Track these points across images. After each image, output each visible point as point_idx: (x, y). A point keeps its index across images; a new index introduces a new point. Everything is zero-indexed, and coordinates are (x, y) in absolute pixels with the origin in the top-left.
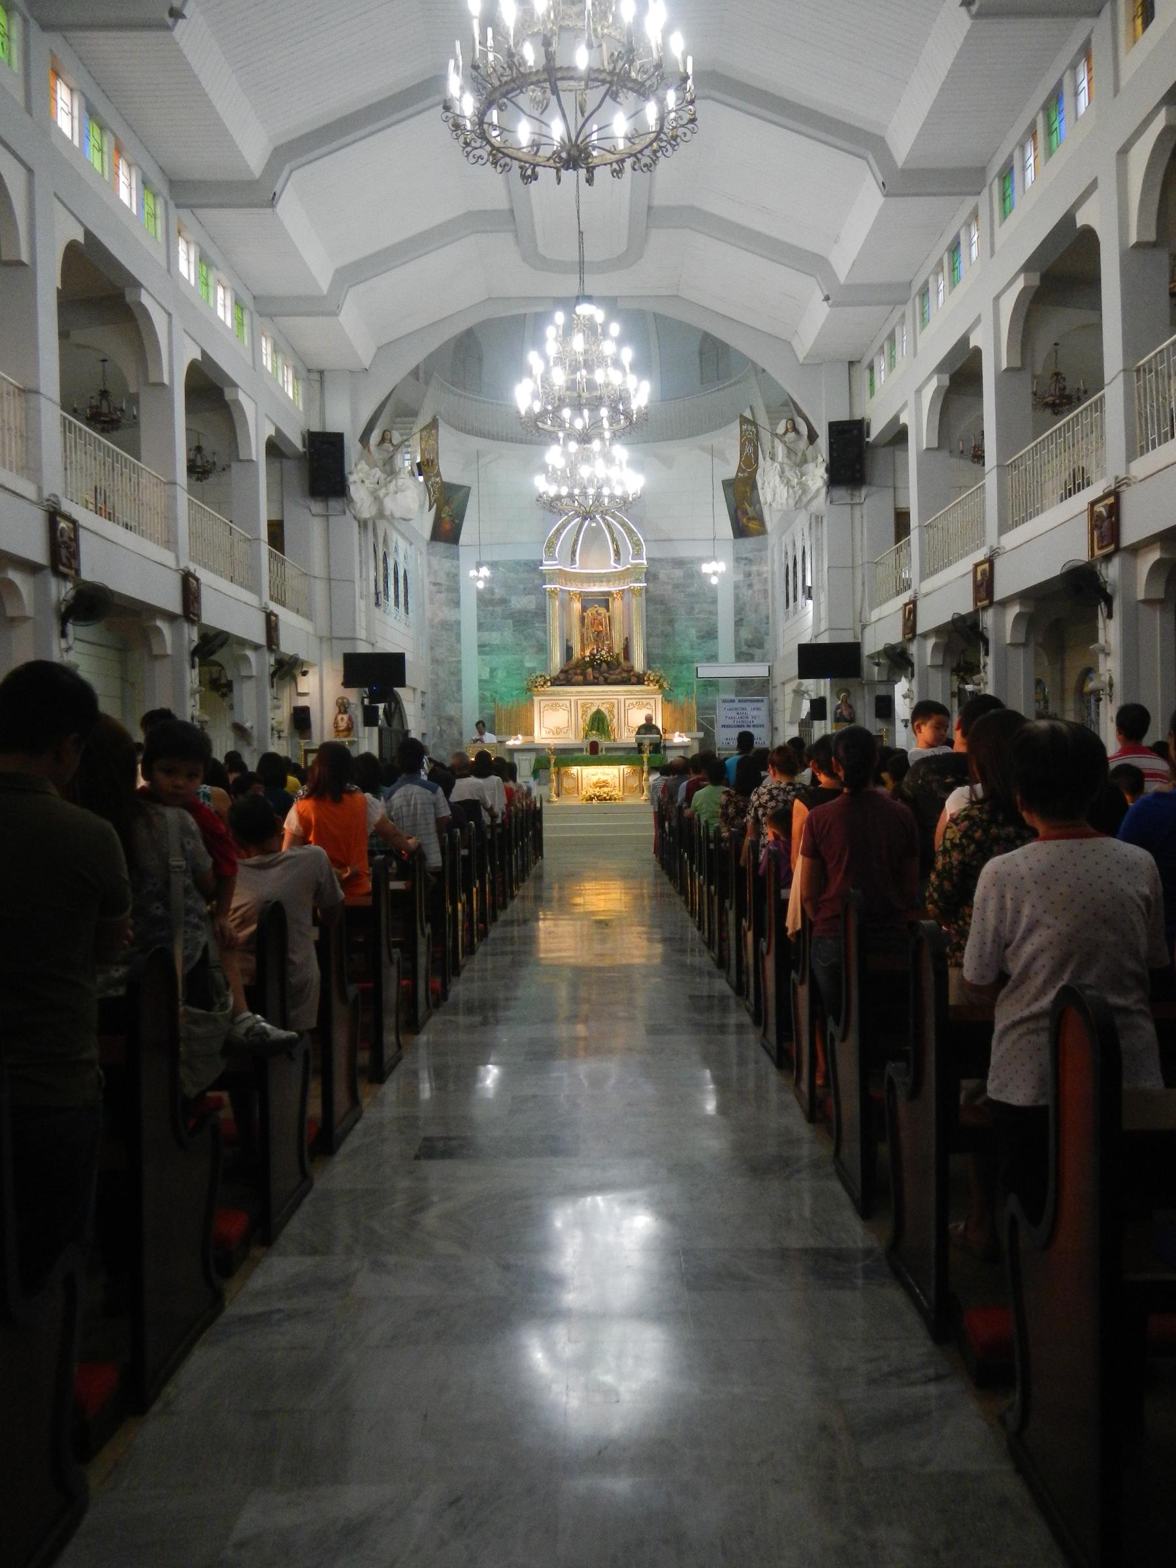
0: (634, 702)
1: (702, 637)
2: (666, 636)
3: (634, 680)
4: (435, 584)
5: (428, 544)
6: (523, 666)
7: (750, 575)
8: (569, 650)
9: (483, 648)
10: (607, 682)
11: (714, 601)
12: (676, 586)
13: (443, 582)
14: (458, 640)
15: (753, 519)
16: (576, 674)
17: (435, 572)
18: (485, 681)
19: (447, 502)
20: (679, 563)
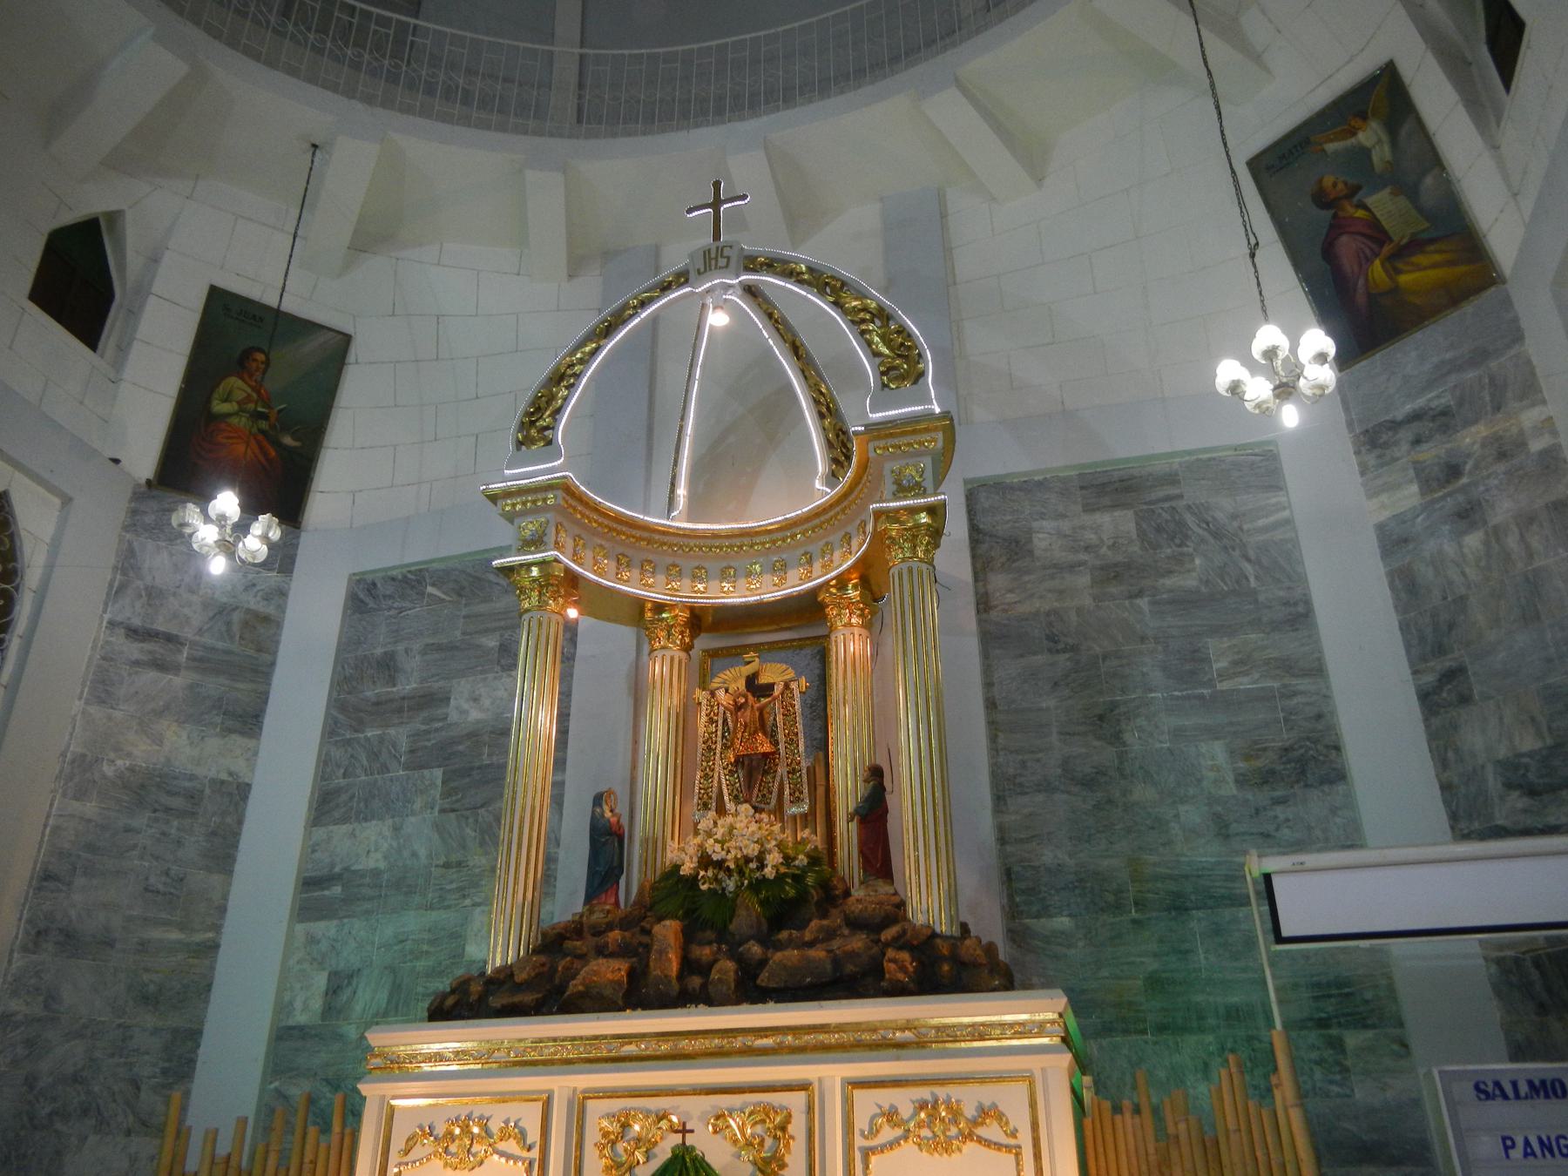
0: (903, 1100)
1: (1267, 778)
2: (1089, 783)
3: (899, 963)
4: (134, 633)
5: (137, 496)
6: (458, 955)
7: (1453, 471)
8: (607, 844)
9: (318, 892)
10: (750, 991)
11: (1299, 616)
12: (1111, 573)
13: (188, 633)
14: (222, 852)
15: (1416, 245)
16: (601, 951)
17: (154, 595)
18: (302, 1032)
19: (241, 364)
20: (1111, 487)
